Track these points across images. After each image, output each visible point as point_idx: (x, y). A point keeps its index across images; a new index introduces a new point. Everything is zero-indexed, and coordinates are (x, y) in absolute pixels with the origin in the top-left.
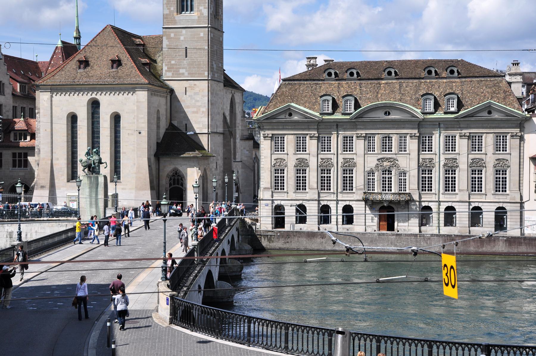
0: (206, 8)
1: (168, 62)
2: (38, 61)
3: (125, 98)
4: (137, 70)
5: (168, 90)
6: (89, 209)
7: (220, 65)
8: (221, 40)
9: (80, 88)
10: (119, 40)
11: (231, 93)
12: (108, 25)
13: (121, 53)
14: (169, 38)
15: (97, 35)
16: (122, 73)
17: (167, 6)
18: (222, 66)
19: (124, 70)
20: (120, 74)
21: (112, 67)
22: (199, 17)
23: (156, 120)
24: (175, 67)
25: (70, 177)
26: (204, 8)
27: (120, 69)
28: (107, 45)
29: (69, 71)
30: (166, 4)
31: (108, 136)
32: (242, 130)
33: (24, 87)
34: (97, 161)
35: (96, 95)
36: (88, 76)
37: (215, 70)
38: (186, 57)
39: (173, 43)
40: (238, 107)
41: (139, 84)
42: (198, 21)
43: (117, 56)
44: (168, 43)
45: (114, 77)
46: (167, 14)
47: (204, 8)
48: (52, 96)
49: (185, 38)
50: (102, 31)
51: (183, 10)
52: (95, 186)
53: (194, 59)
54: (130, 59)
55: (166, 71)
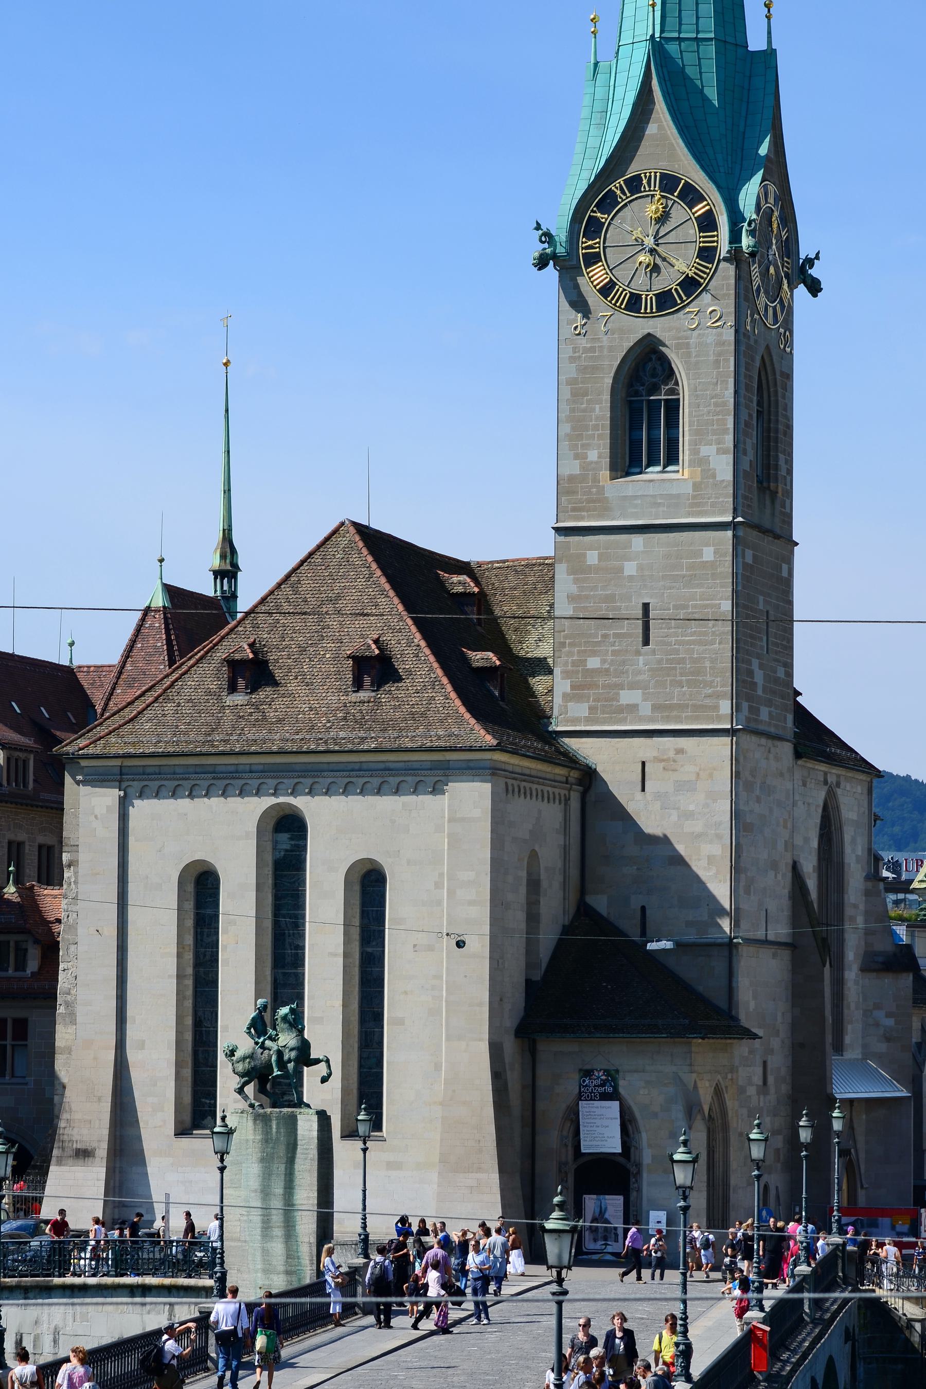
0: (725, 452)
1: (574, 663)
2: (76, 663)
4: (453, 695)
5: (575, 774)
6: (258, 1245)
7: (781, 672)
8: (785, 574)
9: (232, 768)
11: (826, 782)
12: (342, 524)
14: (579, 569)
15: (302, 562)
16: (395, 707)
17: (573, 447)
18: (790, 675)
21: (358, 685)
22: (696, 486)
23: (523, 890)
24: (601, 681)
25: (187, 1117)
26: (720, 451)
28: (338, 597)
29: (189, 701)
30: (569, 437)
31: (335, 955)
32: (868, 932)
33: (20, 764)
34: (293, 1054)
37: (760, 692)
38: (646, 642)
40: (854, 840)
41: (461, 750)
42: (696, 504)
43: (376, 641)
44: (574, 589)
45: (360, 723)
46: (572, 478)
47: (720, 451)
49: (640, 568)
50: (319, 547)
52: (281, 1151)
53: (677, 652)
54: (427, 651)
55: (565, 696)
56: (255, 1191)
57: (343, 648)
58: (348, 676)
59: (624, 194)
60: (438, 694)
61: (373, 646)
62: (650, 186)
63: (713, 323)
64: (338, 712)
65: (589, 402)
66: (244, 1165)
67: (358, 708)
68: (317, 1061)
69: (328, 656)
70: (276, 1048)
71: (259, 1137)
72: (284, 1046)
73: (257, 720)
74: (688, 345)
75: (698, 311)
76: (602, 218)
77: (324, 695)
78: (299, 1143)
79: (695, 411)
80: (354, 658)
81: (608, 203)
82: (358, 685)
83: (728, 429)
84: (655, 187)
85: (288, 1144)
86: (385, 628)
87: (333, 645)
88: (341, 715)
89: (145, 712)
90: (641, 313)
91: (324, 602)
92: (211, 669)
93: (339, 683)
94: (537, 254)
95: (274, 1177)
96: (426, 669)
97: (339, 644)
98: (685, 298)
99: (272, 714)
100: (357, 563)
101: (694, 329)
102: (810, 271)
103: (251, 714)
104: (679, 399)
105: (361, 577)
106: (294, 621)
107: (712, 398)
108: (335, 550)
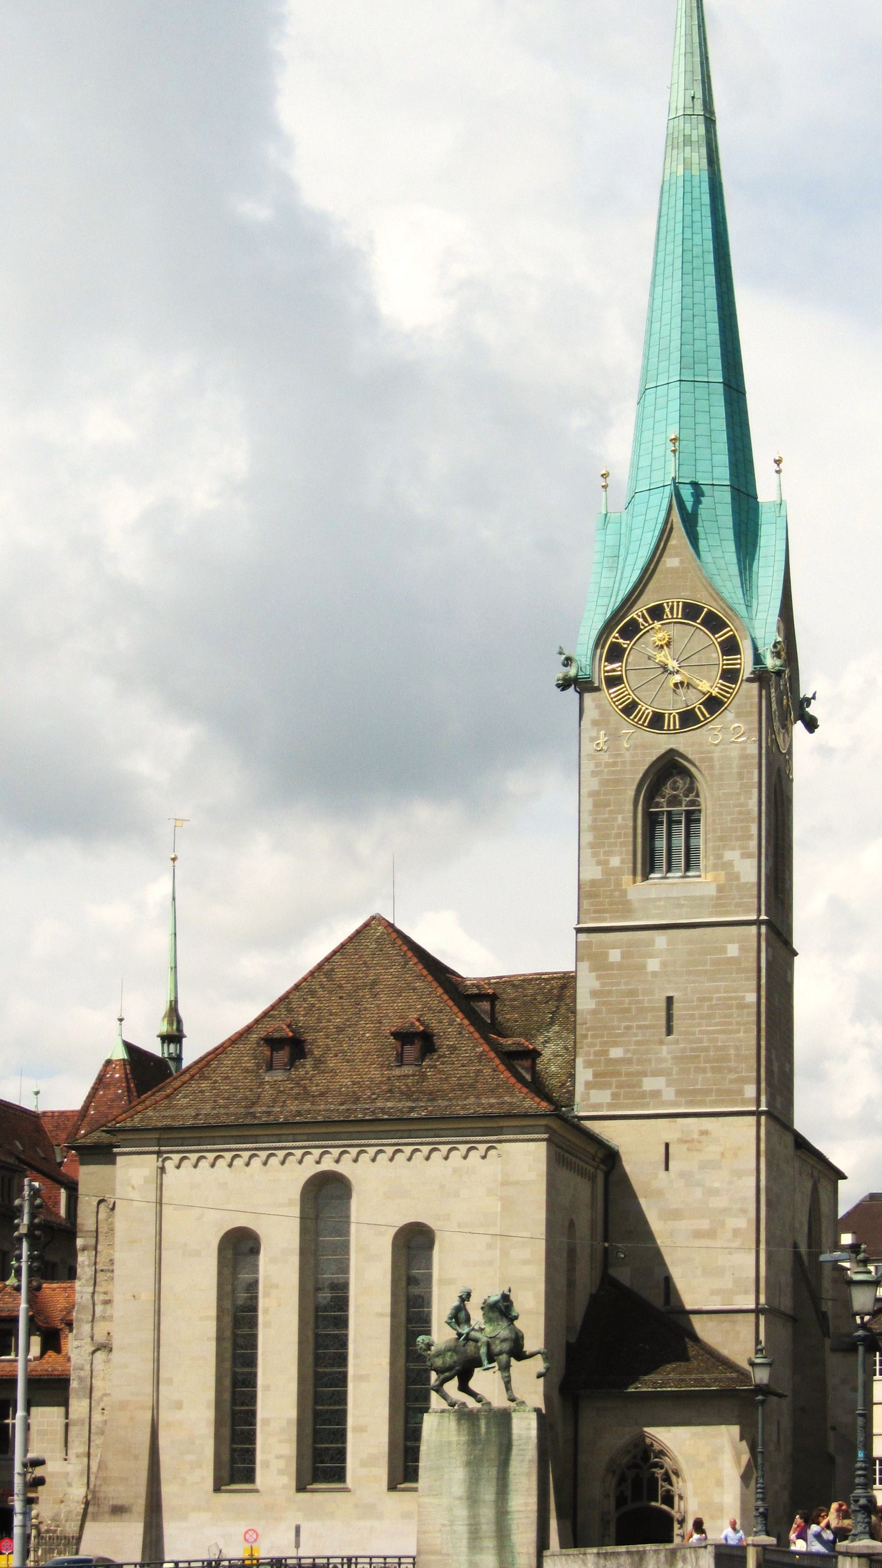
3: (455, 1171)
10: (420, 966)
13: (430, 1009)
17: (595, 854)
19: (447, 1068)
20: (433, 1081)
21: (400, 1060)
27: (430, 1067)
30: (592, 846)
34: (506, 1346)
35: (337, 1161)
36: (305, 1095)
39: (618, 984)
45: (408, 1095)
48: (162, 1170)
51: (652, 869)
52: (493, 1452)
54: (472, 1029)
56: (460, 1498)
57: (383, 1028)
58: (390, 1053)
59: (646, 621)
60: (485, 1067)
61: (417, 1024)
62: (672, 613)
63: (736, 739)
64: (382, 1085)
65: (611, 812)
66: (446, 1470)
67: (404, 1081)
68: (532, 1355)
69: (367, 1035)
70: (484, 1339)
71: (464, 1438)
72: (494, 1337)
73: (299, 1094)
74: (711, 759)
75: (722, 728)
76: (624, 644)
77: (366, 1070)
78: (515, 1443)
79: (719, 819)
80: (396, 1035)
81: (631, 630)
82: (400, 1060)
83: (752, 835)
84: (677, 614)
85: (501, 1445)
86: (425, 1009)
87: (372, 1025)
88: (385, 1087)
89: (181, 1089)
90: (664, 730)
91: (360, 987)
92: (248, 1048)
93: (380, 1059)
94: (561, 675)
95: (483, 1482)
96: (471, 1045)
97: (378, 1025)
98: (708, 716)
99: (314, 1088)
100: (391, 952)
101: (717, 745)
102: (807, 709)
103: (292, 1089)
104: (700, 811)
105: (397, 964)
106: (330, 1004)
107: (736, 806)
108: (368, 941)
